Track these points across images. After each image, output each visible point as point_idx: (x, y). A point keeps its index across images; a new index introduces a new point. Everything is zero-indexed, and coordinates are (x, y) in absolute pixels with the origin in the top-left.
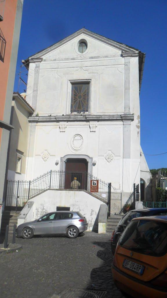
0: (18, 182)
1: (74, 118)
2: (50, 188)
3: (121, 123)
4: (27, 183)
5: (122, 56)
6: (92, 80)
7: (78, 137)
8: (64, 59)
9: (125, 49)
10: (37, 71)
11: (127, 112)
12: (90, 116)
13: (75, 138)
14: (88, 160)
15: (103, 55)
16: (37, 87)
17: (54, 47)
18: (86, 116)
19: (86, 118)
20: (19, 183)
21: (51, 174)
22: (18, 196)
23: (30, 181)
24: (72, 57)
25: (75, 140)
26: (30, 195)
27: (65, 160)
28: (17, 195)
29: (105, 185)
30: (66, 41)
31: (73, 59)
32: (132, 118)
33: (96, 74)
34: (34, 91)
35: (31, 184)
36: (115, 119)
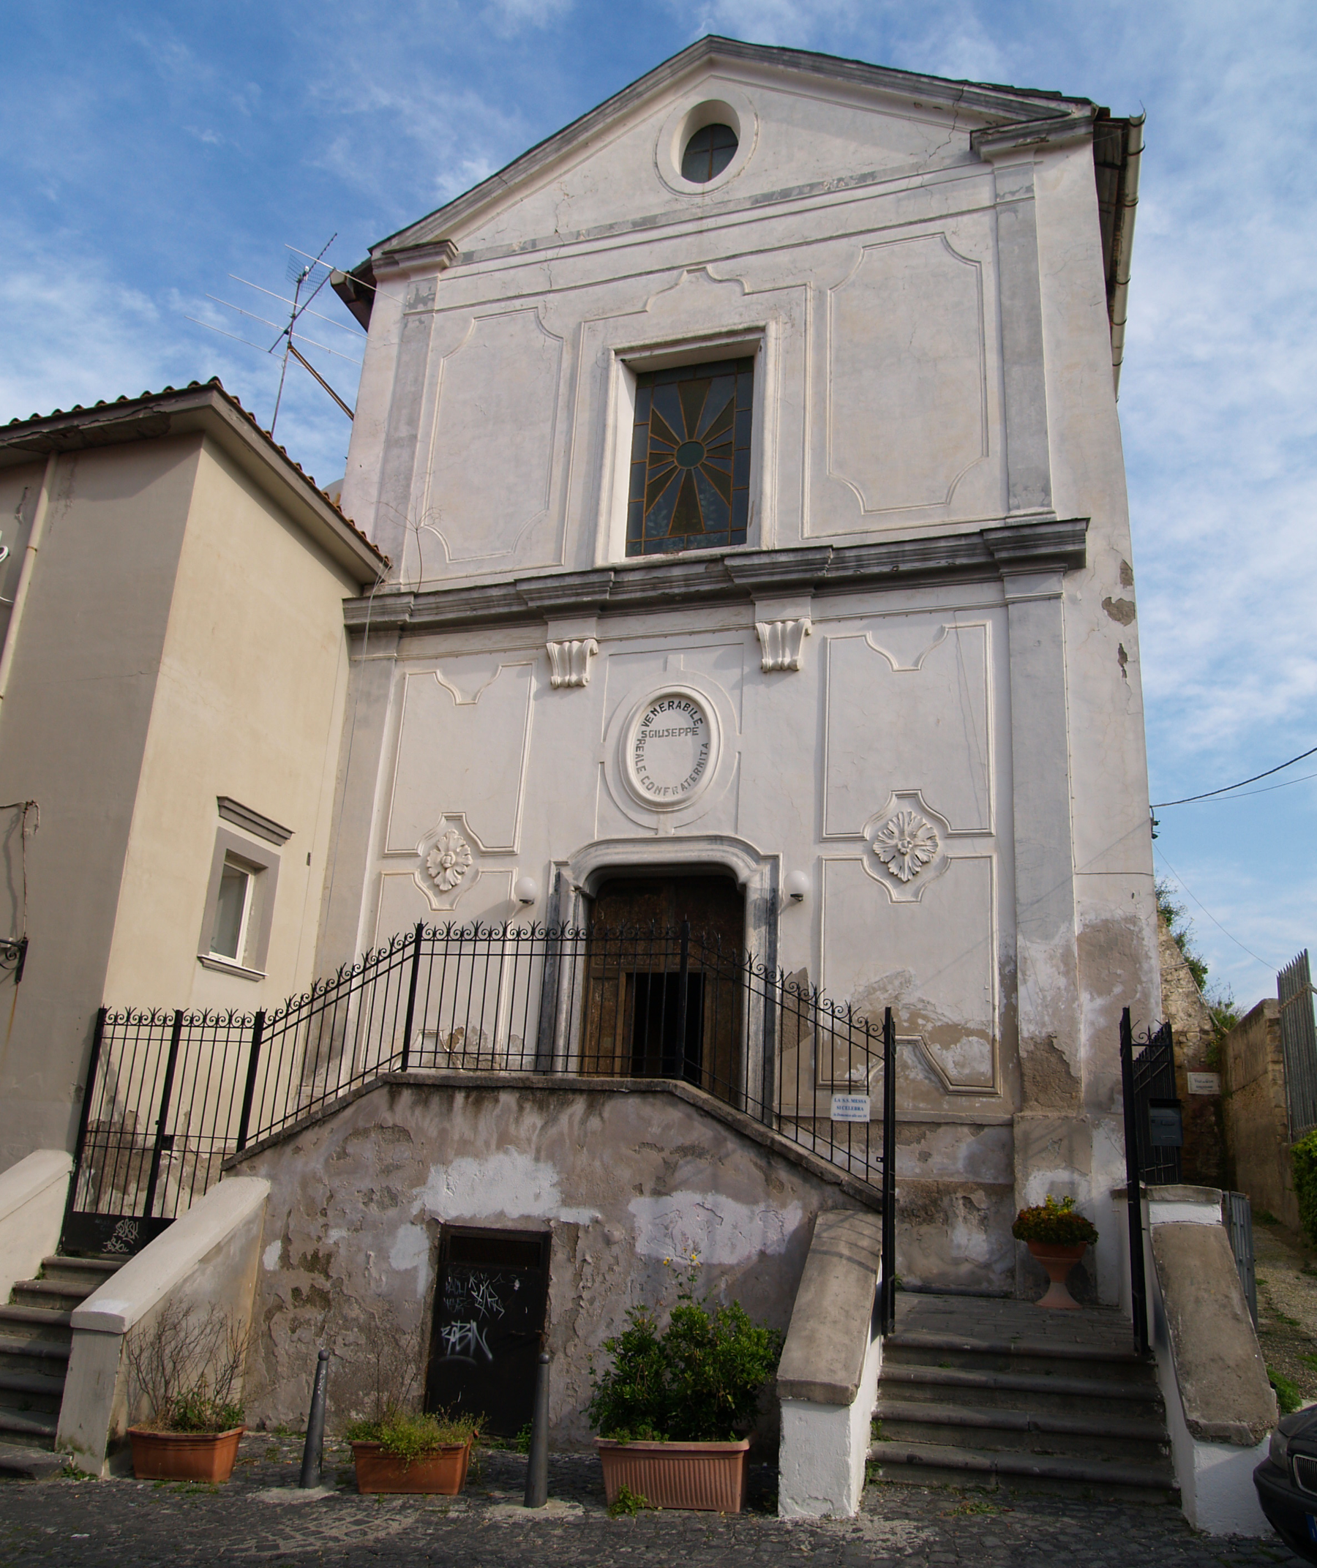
0: (177, 1027)
1: (643, 585)
2: (404, 1066)
3: (985, 593)
4: (235, 1034)
5: (975, 155)
6: (773, 330)
7: (673, 718)
8: (589, 232)
9: (993, 111)
10: (421, 322)
11: (1025, 512)
12: (756, 560)
13: (652, 726)
14: (744, 868)
15: (843, 174)
16: (413, 421)
17: (525, 170)
18: (728, 562)
19: (728, 574)
20: (184, 1032)
21: (416, 956)
22: (169, 1131)
23: (260, 1016)
24: (637, 216)
25: (657, 734)
26: (251, 1131)
27: (576, 879)
28: (161, 1123)
29: (859, 1038)
30: (600, 126)
31: (646, 224)
32: (1070, 548)
33: (795, 293)
34: (391, 443)
35: (266, 1034)
36: (943, 563)
